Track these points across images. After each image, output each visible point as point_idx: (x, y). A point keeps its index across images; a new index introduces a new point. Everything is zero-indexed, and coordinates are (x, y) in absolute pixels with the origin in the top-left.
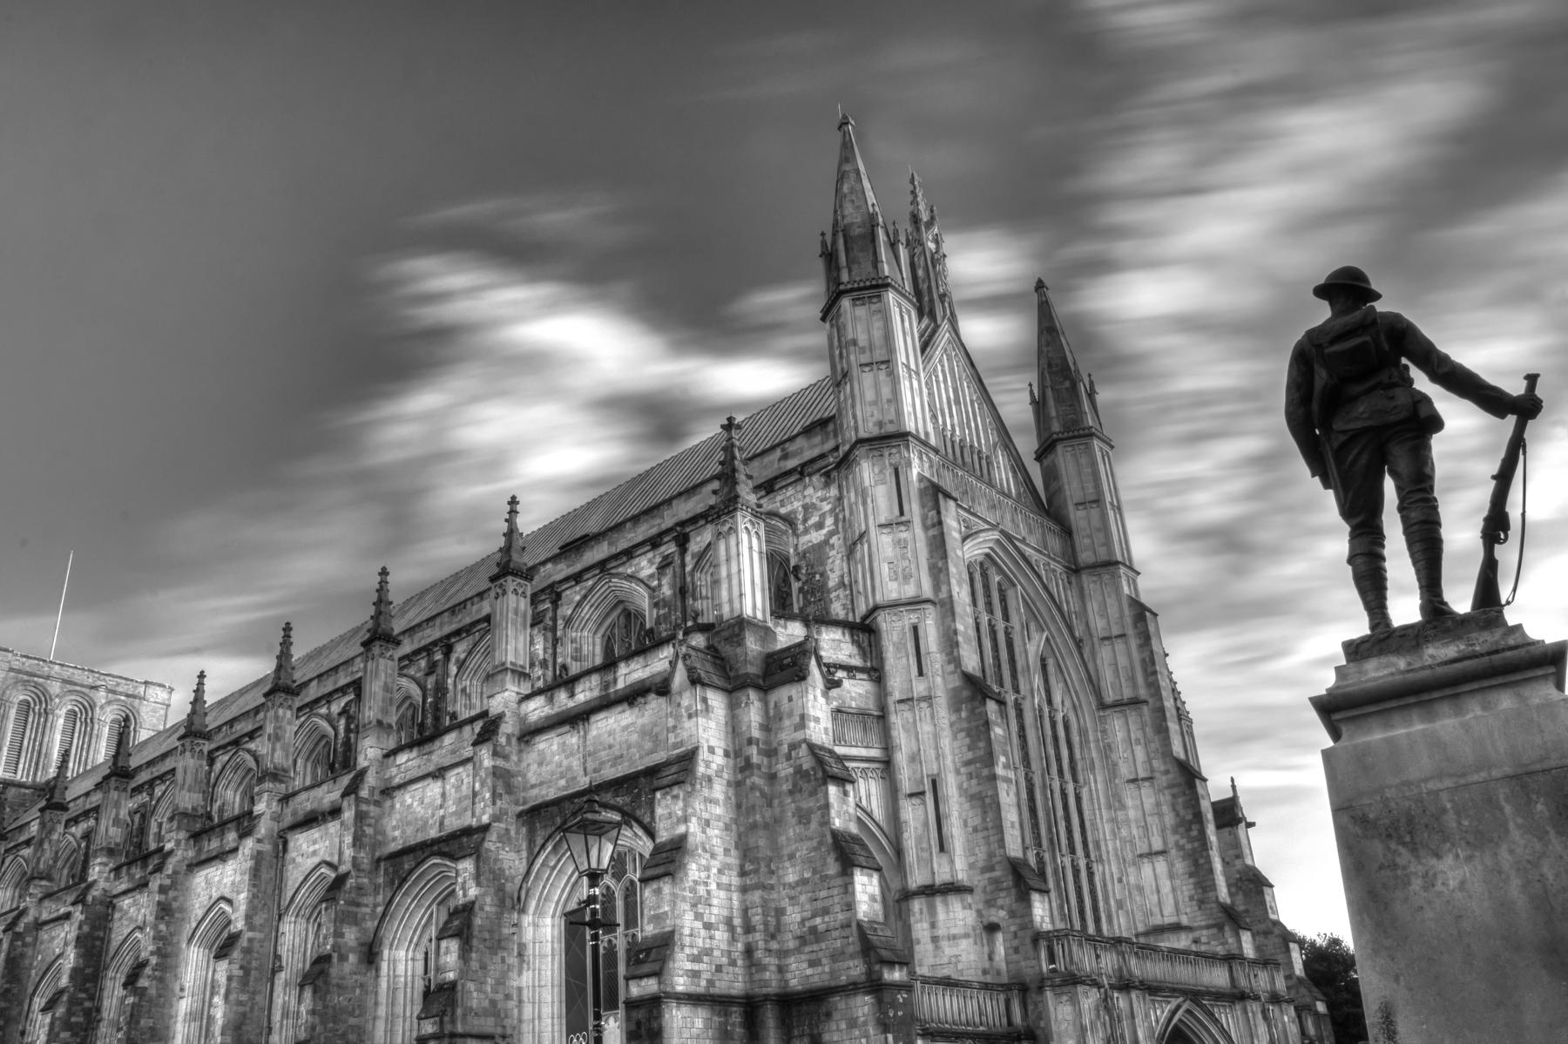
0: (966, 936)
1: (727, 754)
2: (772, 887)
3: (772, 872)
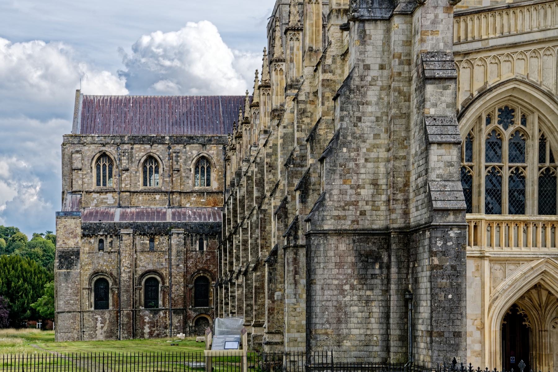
2: (404, 158)
3: (406, 147)
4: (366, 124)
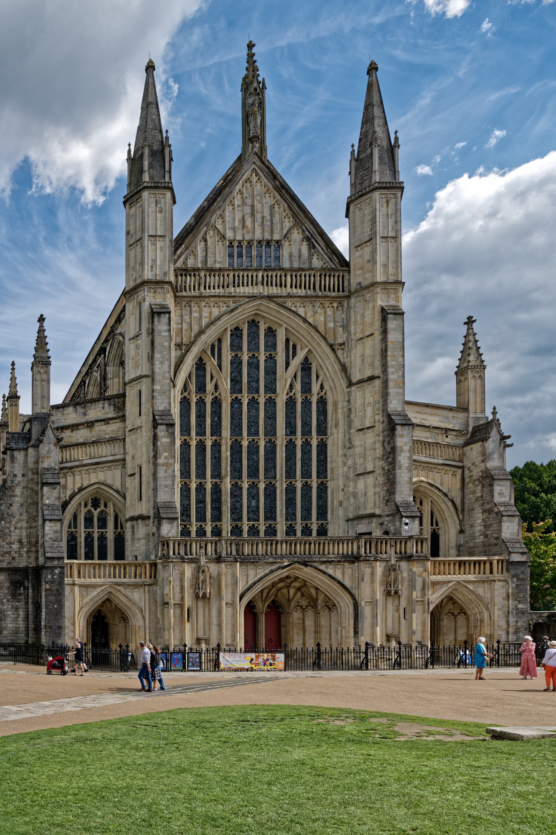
0: (143, 539)
1: (23, 476)
2: (36, 527)
3: (36, 521)
4: (15, 508)
